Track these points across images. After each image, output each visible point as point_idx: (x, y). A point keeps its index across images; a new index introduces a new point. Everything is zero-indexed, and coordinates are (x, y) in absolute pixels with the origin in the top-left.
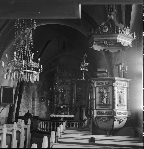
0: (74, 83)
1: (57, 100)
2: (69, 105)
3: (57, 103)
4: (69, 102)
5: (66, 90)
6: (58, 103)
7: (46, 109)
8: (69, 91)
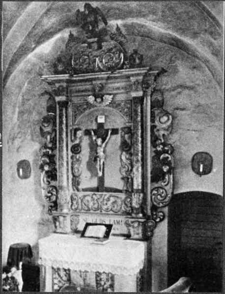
0: (140, 94)
1: (74, 176)
2: (120, 191)
3: (76, 183)
4: (123, 179)
5: (107, 130)
6: (78, 184)
7: (40, 209)
8: (120, 132)
